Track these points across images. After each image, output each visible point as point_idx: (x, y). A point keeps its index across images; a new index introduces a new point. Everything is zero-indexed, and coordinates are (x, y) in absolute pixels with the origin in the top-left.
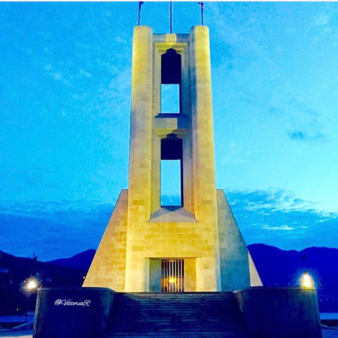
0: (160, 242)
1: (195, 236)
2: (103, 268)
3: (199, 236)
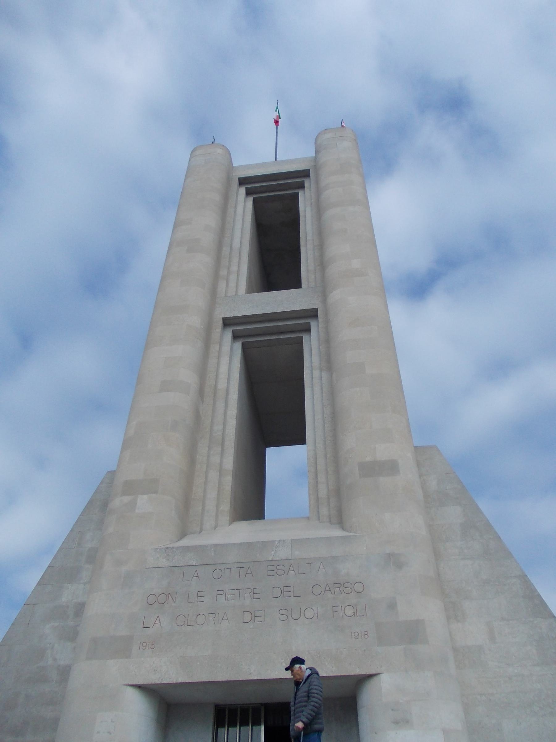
0: (201, 619)
1: (342, 586)
3: (358, 587)
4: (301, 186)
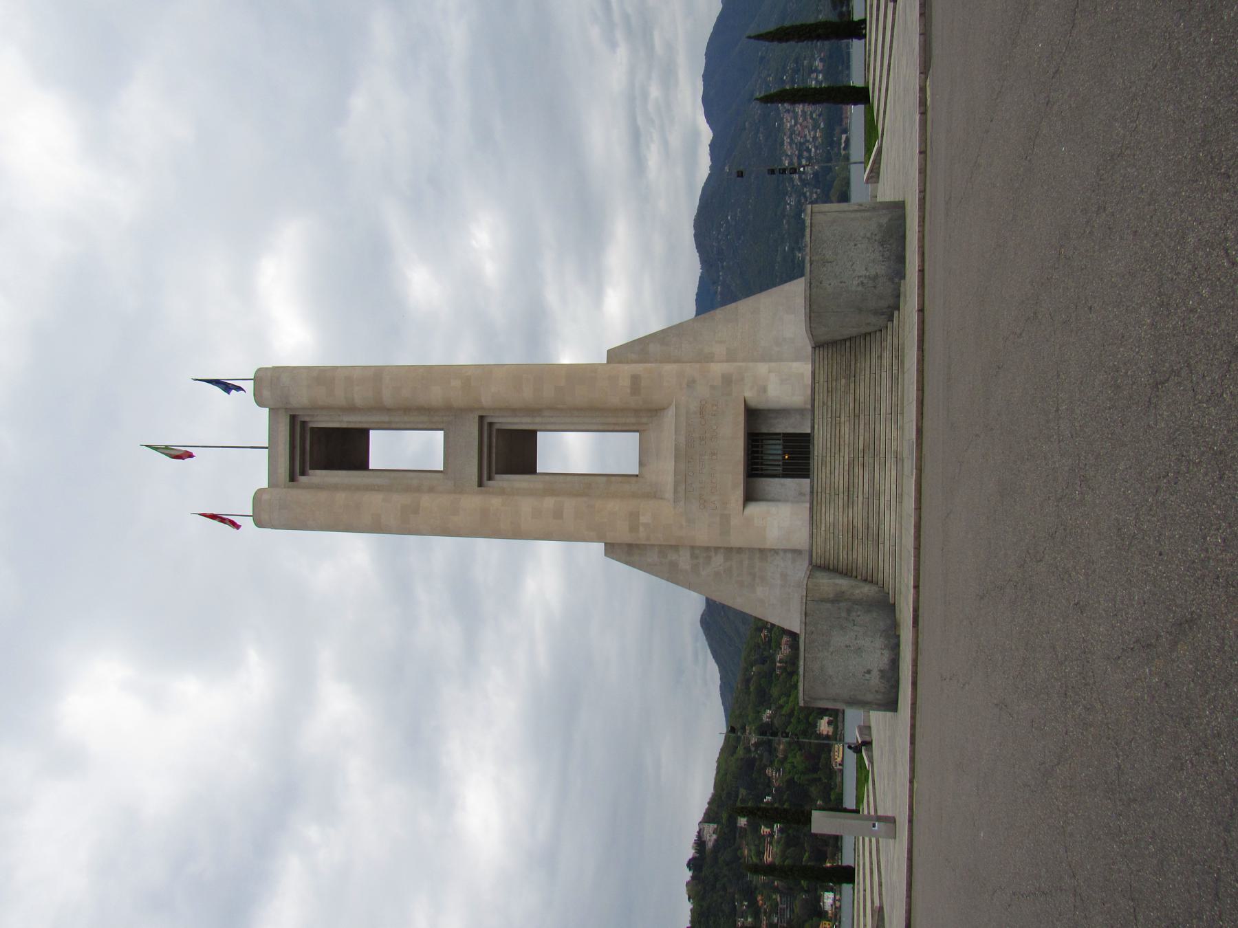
1: (702, 412)
2: (760, 591)
4: (304, 423)
